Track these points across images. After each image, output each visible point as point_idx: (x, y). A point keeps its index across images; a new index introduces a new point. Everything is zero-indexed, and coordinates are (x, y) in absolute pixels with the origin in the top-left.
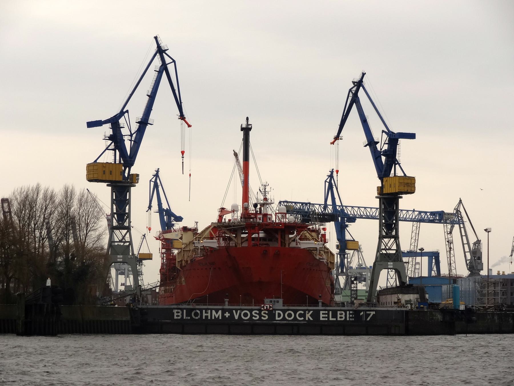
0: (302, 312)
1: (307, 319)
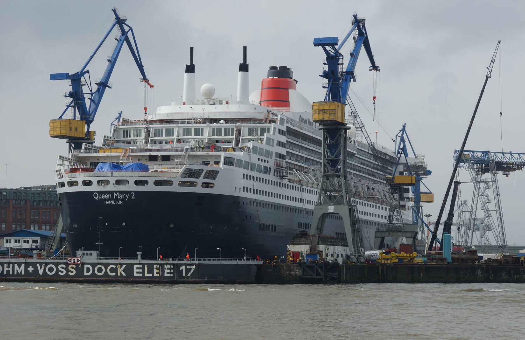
0: (114, 267)
1: (119, 274)
